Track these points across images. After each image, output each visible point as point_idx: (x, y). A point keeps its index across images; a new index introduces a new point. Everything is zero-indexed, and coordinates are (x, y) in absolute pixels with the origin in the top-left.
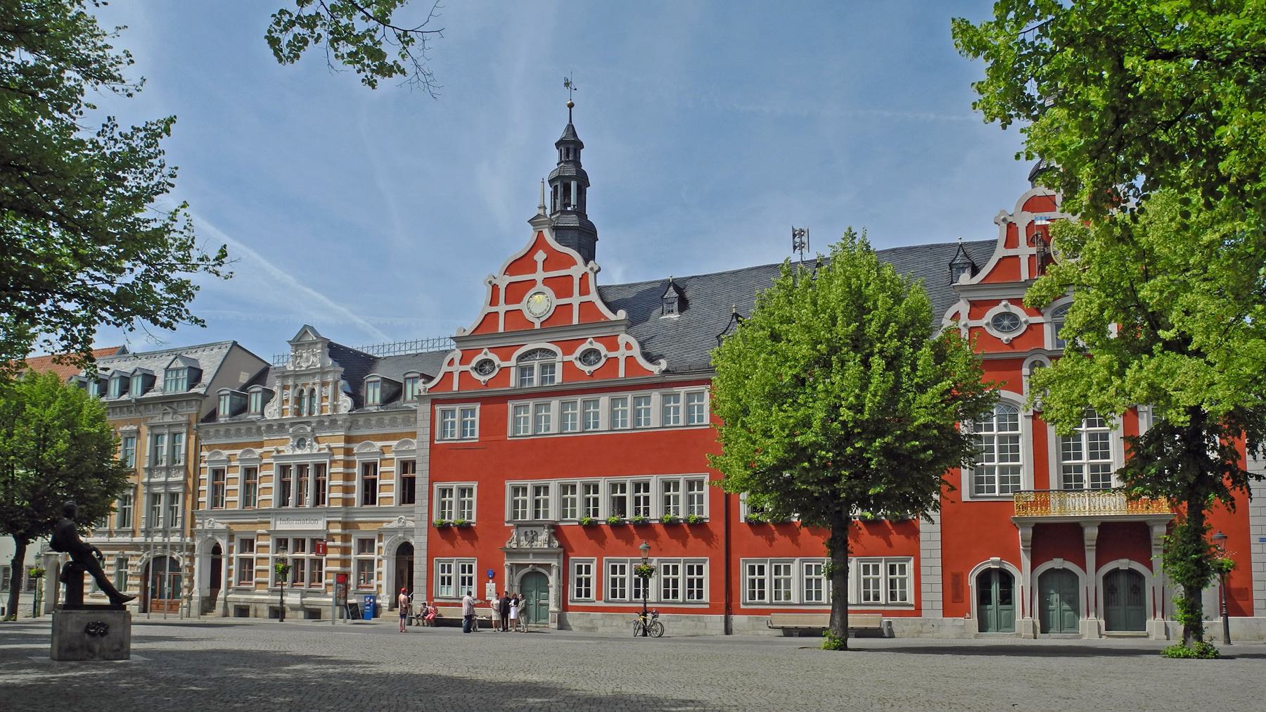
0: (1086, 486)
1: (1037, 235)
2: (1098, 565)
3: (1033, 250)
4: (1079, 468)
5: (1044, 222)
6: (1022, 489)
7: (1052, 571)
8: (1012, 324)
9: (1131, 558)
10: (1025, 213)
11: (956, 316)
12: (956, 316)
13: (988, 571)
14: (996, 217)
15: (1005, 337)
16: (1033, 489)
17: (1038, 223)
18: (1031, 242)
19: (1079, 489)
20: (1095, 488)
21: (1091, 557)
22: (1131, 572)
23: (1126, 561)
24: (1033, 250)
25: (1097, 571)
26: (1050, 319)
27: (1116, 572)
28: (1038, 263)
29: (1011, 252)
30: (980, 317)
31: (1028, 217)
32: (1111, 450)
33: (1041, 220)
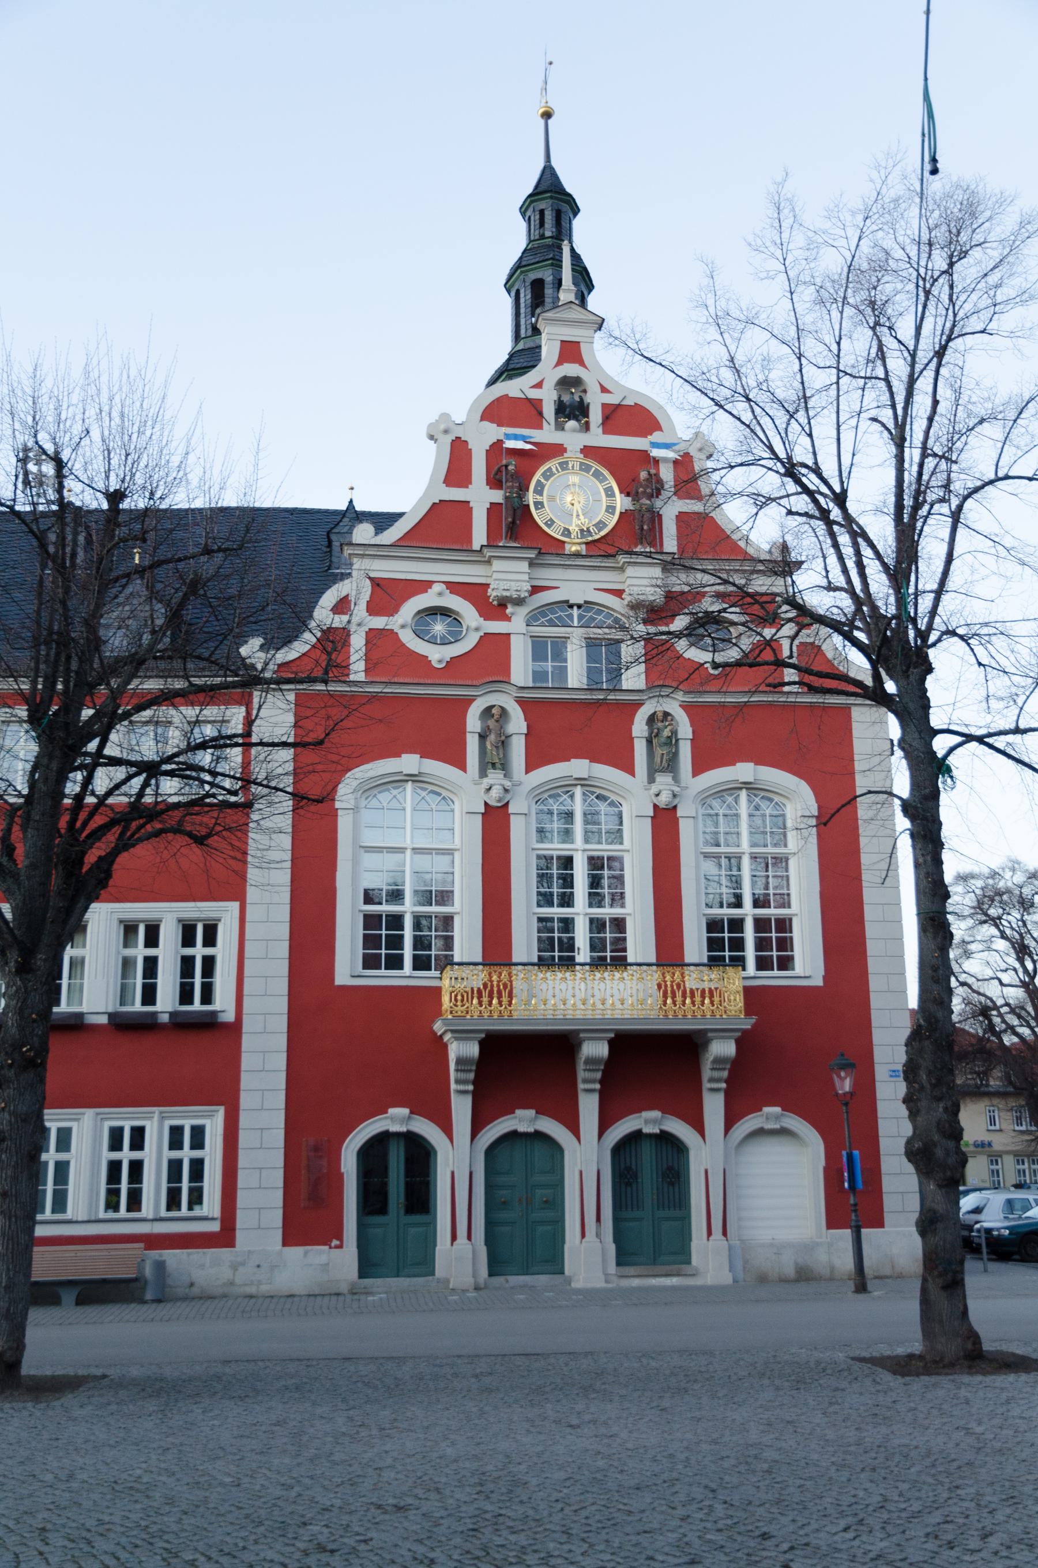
0: (579, 959)
1: (506, 466)
2: (604, 1125)
3: (498, 496)
4: (567, 924)
5: (520, 445)
6: (456, 959)
7: (513, 1136)
8: (450, 633)
9: (668, 1110)
10: (486, 424)
11: (342, 606)
12: (342, 606)
13: (383, 1139)
14: (430, 425)
15: (437, 655)
16: (479, 959)
17: (510, 444)
18: (494, 481)
19: (568, 963)
20: (598, 963)
21: (589, 1107)
22: (665, 1138)
23: (656, 1114)
24: (498, 496)
25: (601, 1135)
26: (522, 628)
27: (636, 1136)
28: (506, 519)
29: (456, 494)
30: (392, 611)
31: (493, 432)
32: (628, 890)
33: (516, 437)
